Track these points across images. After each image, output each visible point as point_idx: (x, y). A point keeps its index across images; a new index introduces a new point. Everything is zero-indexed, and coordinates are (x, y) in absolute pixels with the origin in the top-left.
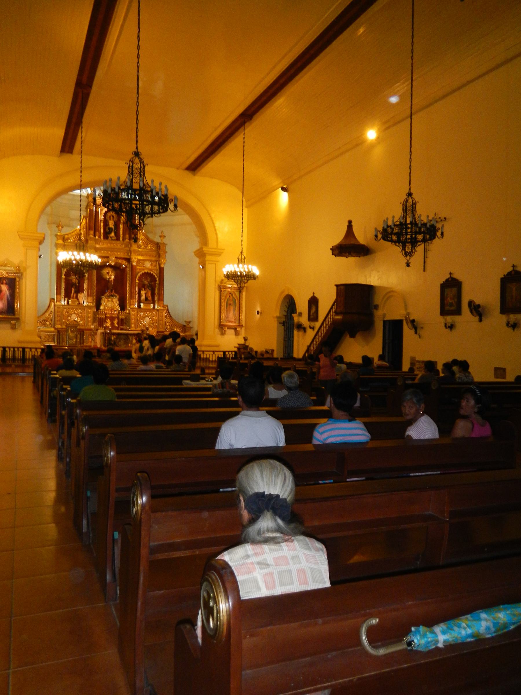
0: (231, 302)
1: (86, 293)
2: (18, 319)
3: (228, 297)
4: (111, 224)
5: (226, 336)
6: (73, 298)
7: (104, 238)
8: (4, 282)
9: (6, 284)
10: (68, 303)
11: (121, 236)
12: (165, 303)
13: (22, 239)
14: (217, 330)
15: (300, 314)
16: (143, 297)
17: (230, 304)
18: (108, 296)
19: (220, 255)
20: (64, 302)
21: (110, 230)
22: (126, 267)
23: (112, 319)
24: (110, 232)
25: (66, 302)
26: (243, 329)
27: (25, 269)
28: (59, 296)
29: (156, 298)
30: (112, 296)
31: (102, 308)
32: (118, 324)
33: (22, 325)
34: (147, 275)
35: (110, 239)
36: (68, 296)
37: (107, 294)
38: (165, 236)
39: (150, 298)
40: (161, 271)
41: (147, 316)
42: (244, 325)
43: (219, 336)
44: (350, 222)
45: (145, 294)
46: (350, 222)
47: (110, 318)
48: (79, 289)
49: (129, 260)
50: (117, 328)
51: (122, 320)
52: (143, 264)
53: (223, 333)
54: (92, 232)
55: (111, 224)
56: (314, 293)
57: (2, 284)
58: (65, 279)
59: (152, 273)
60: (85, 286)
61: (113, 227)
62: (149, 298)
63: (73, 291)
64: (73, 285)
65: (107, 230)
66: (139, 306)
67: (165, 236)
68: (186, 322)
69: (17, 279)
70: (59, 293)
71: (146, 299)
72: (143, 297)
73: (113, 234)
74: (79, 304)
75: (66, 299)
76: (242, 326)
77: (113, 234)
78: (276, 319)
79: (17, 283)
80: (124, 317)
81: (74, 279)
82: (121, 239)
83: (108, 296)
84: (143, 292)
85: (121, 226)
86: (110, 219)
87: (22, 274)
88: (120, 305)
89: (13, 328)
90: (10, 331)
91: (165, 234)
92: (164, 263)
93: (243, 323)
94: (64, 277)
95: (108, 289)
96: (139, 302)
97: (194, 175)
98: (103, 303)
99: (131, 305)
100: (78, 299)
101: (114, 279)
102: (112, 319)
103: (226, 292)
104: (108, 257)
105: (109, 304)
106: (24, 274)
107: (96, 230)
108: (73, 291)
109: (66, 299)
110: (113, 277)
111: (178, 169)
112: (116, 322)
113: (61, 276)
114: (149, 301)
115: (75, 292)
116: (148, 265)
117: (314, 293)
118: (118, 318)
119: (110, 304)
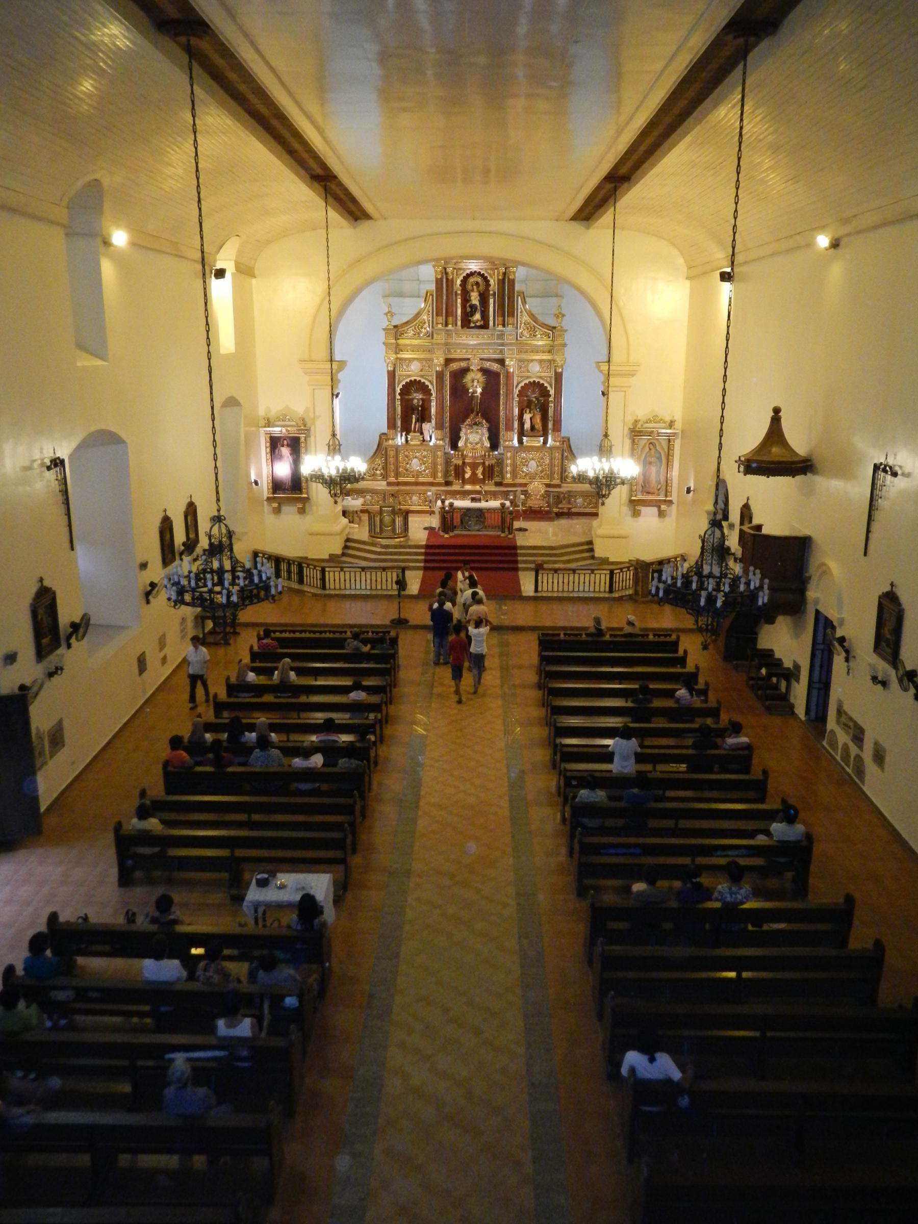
0: (653, 460)
1: (433, 421)
2: (308, 499)
3: (647, 449)
4: (475, 299)
5: (641, 519)
6: (415, 432)
7: (463, 327)
8: (285, 442)
9: (288, 445)
10: (407, 441)
11: (491, 318)
12: (564, 432)
13: (306, 373)
14: (626, 510)
15: (731, 526)
16: (527, 426)
17: (650, 463)
18: (470, 425)
19: (633, 375)
20: (400, 440)
21: (473, 307)
23: (474, 467)
24: (472, 314)
25: (403, 438)
26: (674, 507)
27: (314, 421)
28: (392, 431)
29: (550, 425)
30: (475, 424)
31: (460, 444)
32: (483, 473)
33: (314, 508)
35: (472, 325)
36: (406, 429)
37: (468, 421)
38: (563, 316)
39: (539, 425)
41: (533, 459)
42: (675, 501)
43: (629, 520)
44: (777, 411)
45: (531, 419)
46: (777, 411)
47: (469, 464)
48: (424, 417)
49: (502, 362)
50: (482, 481)
51: (491, 468)
52: (527, 366)
53: (636, 514)
54: (441, 319)
56: (748, 499)
57: (283, 446)
58: (401, 400)
59: (542, 382)
61: (478, 303)
62: (537, 427)
65: (468, 309)
66: (520, 442)
67: (563, 316)
69: (302, 440)
70: (391, 424)
71: (533, 428)
72: (527, 426)
73: (477, 316)
74: (424, 441)
76: (671, 502)
77: (477, 316)
78: (706, 515)
79: (303, 445)
80: (493, 462)
81: (417, 397)
82: (491, 323)
83: (470, 425)
84: (527, 417)
85: (491, 301)
86: (473, 290)
87: (309, 430)
88: (490, 438)
89: (302, 511)
90: (298, 516)
91: (563, 312)
92: (562, 367)
93: (674, 497)
95: (472, 411)
96: (521, 433)
97: (588, 228)
100: (422, 433)
101: (481, 394)
102: (474, 467)
103: (642, 443)
104: (468, 359)
106: (312, 429)
107: (449, 313)
110: (479, 390)
111: (557, 220)
112: (480, 471)
114: (538, 431)
115: (417, 420)
116: (535, 368)
117: (748, 499)
118: (484, 463)
119: (474, 438)
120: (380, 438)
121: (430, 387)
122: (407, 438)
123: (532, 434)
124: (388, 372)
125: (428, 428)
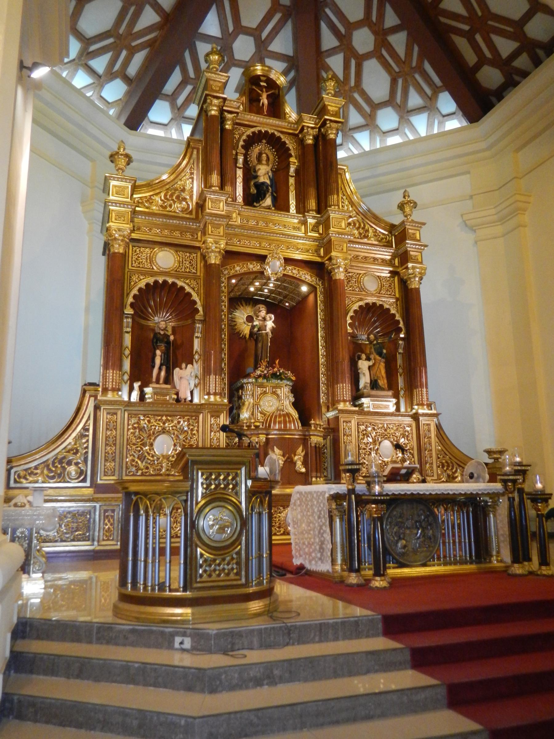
4: (264, 173)
6: (158, 382)
16: (364, 380)
22: (313, 289)
30: (275, 376)
32: (305, 463)
34: (371, 312)
36: (140, 374)
39: (383, 382)
40: (409, 299)
45: (370, 368)
48: (177, 355)
49: (320, 269)
55: (264, 173)
58: (133, 316)
60: (197, 345)
61: (268, 182)
63: (158, 361)
64: (159, 339)
65: (253, 190)
68: (489, 452)
70: (111, 358)
71: (374, 385)
73: (268, 201)
75: (136, 385)
77: (268, 201)
84: (363, 365)
85: (292, 181)
88: (295, 405)
94: (129, 311)
101: (273, 330)
104: (262, 259)
105: (269, 404)
108: (158, 361)
109: (136, 385)
112: (298, 458)
120: (84, 392)
121: (195, 297)
123: (374, 392)
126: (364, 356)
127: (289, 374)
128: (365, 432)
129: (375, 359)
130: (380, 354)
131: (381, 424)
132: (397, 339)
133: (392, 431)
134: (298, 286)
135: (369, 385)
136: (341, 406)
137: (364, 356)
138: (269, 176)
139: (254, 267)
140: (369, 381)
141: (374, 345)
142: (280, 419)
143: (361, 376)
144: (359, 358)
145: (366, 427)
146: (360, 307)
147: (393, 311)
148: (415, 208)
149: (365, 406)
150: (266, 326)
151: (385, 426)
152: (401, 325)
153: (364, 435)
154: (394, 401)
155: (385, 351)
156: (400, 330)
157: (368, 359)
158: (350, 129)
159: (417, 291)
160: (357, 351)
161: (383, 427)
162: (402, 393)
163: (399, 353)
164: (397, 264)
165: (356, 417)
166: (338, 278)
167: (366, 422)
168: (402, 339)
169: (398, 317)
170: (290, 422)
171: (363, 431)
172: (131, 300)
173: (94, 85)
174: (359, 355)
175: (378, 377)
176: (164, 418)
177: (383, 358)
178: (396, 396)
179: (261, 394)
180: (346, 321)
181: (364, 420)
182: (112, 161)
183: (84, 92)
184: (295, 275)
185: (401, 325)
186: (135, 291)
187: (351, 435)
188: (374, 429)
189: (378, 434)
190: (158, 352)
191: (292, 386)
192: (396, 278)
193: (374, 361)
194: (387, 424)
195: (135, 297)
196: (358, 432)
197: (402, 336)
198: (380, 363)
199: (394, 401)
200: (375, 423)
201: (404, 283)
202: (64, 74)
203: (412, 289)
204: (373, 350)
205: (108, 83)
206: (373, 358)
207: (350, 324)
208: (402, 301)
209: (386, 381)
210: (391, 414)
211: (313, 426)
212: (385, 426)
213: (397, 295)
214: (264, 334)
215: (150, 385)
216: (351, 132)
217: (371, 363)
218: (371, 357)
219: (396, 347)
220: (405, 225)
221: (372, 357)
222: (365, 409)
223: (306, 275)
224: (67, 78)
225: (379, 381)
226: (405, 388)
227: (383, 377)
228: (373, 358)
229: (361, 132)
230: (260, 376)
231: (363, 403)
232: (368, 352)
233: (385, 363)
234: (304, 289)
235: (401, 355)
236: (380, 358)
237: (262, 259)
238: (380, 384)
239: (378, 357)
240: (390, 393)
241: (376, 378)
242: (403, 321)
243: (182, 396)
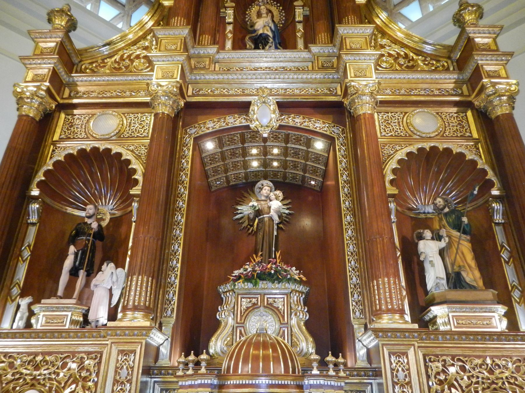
10: (28, 325)
16: (435, 275)
22: (330, 140)
30: (265, 276)
31: (217, 345)
39: (472, 275)
45: (442, 253)
61: (270, 34)
71: (455, 280)
74: (86, 322)
84: (429, 248)
88: (310, 326)
98: (227, 318)
99: (377, 314)
104: (244, 107)
108: (68, 263)
113: (27, 186)
114: (472, 288)
122: (31, 313)
124: (20, 117)
125: (109, 279)
126: (428, 234)
127: (294, 272)
128: (442, 377)
129: (449, 237)
130: (458, 226)
131: (479, 357)
132: (487, 202)
133: (507, 374)
134: (309, 143)
135: (444, 282)
136: (386, 321)
137: (428, 234)
138: (271, 28)
139: (234, 121)
140: (443, 275)
141: (446, 214)
142: (256, 352)
143: (427, 266)
144: (421, 237)
145: (444, 366)
146: (409, 154)
147: (470, 156)
148: (481, 18)
149: (439, 321)
150: (269, 208)
151: (489, 361)
152: (490, 175)
153: (441, 383)
154: (502, 309)
155: (465, 219)
156: (490, 184)
157: (438, 237)
158: (395, 6)
159: (510, 117)
160: (416, 226)
161: (484, 363)
162: (516, 295)
163: (498, 224)
164: (466, 92)
165: (417, 345)
166: (361, 112)
167: (442, 355)
168: (496, 198)
169: (482, 164)
170: (276, 360)
171: (438, 373)
172: (40, 177)
173: (120, 16)
174: (420, 233)
175: (460, 266)
176: (39, 358)
177: (465, 232)
178: (504, 298)
179: (248, 308)
180: (383, 177)
181: (438, 351)
182: (49, 23)
183: (115, 24)
184: (298, 125)
185: (490, 175)
186: (49, 166)
187: (409, 383)
188: (463, 368)
189: (474, 380)
190: (72, 249)
191: (307, 295)
192: (469, 113)
193: (447, 239)
194: (492, 357)
195: (47, 173)
196: (428, 377)
197: (495, 192)
198: (459, 243)
199: (502, 309)
200: (465, 356)
201: (484, 117)
202: (89, 7)
203: (498, 117)
204: (444, 222)
205: (134, 11)
206: (445, 235)
207: (392, 182)
208: (486, 142)
209: (477, 274)
210: (499, 336)
211: (331, 366)
212: (489, 361)
213: (475, 135)
214: (266, 219)
215: (43, 301)
216: (397, 8)
217: (443, 244)
218: (441, 234)
219: (489, 214)
220: (468, 34)
221: (443, 232)
222: (442, 328)
223: (318, 124)
224: (92, 11)
225: (464, 274)
226: (520, 284)
227: (470, 267)
228: (445, 235)
229: (408, 5)
230: (239, 278)
231: (435, 317)
232: (438, 227)
233: (471, 241)
234: (319, 145)
235: (501, 227)
236: (459, 234)
237: (244, 107)
238: (468, 280)
239: (455, 233)
240: (490, 294)
241: (456, 269)
242: (493, 169)
243: (91, 317)
